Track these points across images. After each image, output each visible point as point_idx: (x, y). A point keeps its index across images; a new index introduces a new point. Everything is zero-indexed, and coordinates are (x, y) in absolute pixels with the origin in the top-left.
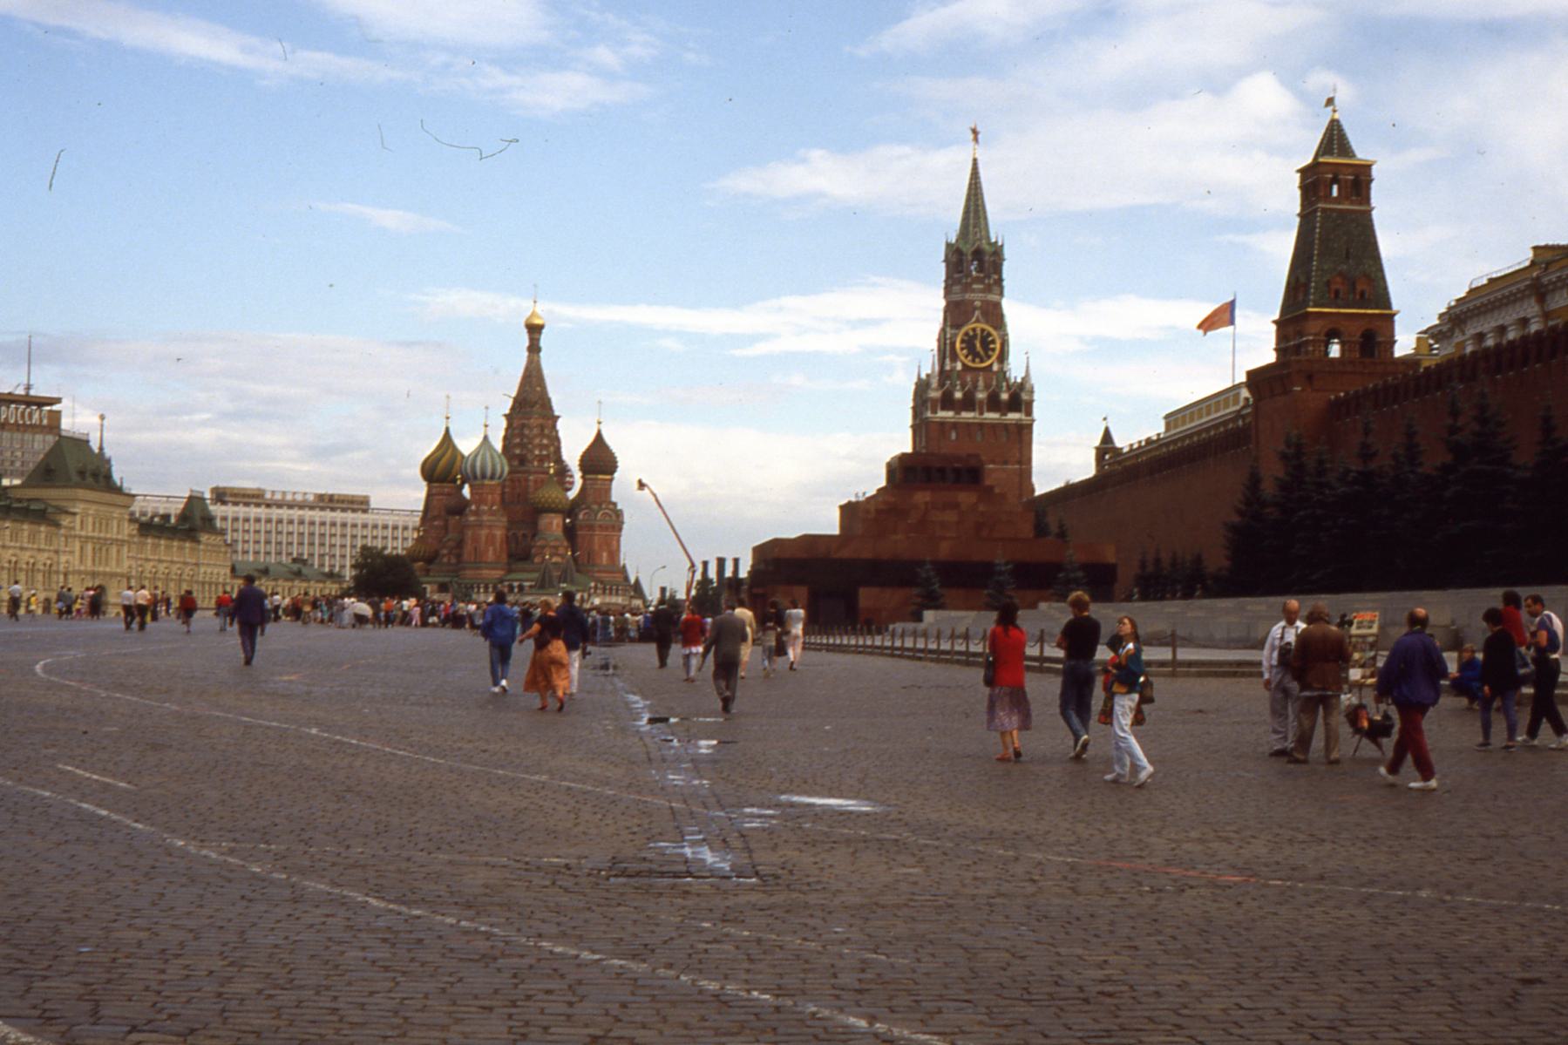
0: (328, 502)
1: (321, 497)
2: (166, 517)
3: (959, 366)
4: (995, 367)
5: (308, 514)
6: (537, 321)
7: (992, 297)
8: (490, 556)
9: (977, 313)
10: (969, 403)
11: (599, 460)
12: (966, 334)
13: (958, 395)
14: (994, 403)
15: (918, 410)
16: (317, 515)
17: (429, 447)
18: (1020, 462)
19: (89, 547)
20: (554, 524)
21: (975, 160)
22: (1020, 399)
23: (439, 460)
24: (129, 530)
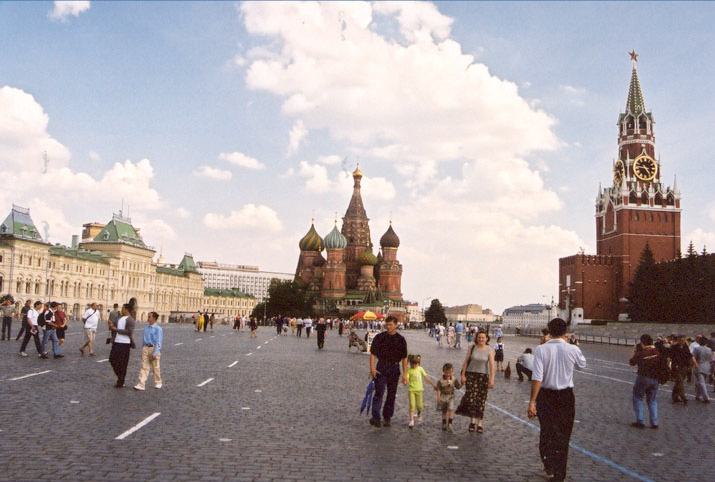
0: (242, 268)
1: (240, 267)
2: (173, 266)
3: (635, 179)
4: (655, 181)
5: (234, 273)
6: (360, 173)
7: (650, 142)
8: (337, 286)
9: (644, 150)
10: (644, 199)
11: (390, 241)
12: (639, 161)
13: (639, 195)
14: (658, 200)
15: (600, 208)
16: (238, 273)
17: (302, 235)
18: (674, 234)
19: (127, 278)
20: (369, 271)
21: (634, 70)
22: (671, 200)
23: (308, 240)
24: (151, 270)
